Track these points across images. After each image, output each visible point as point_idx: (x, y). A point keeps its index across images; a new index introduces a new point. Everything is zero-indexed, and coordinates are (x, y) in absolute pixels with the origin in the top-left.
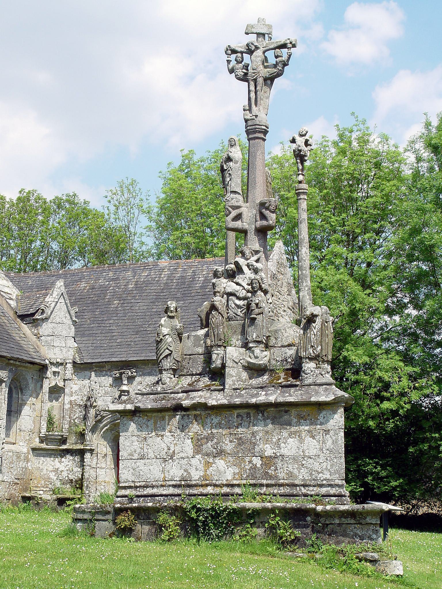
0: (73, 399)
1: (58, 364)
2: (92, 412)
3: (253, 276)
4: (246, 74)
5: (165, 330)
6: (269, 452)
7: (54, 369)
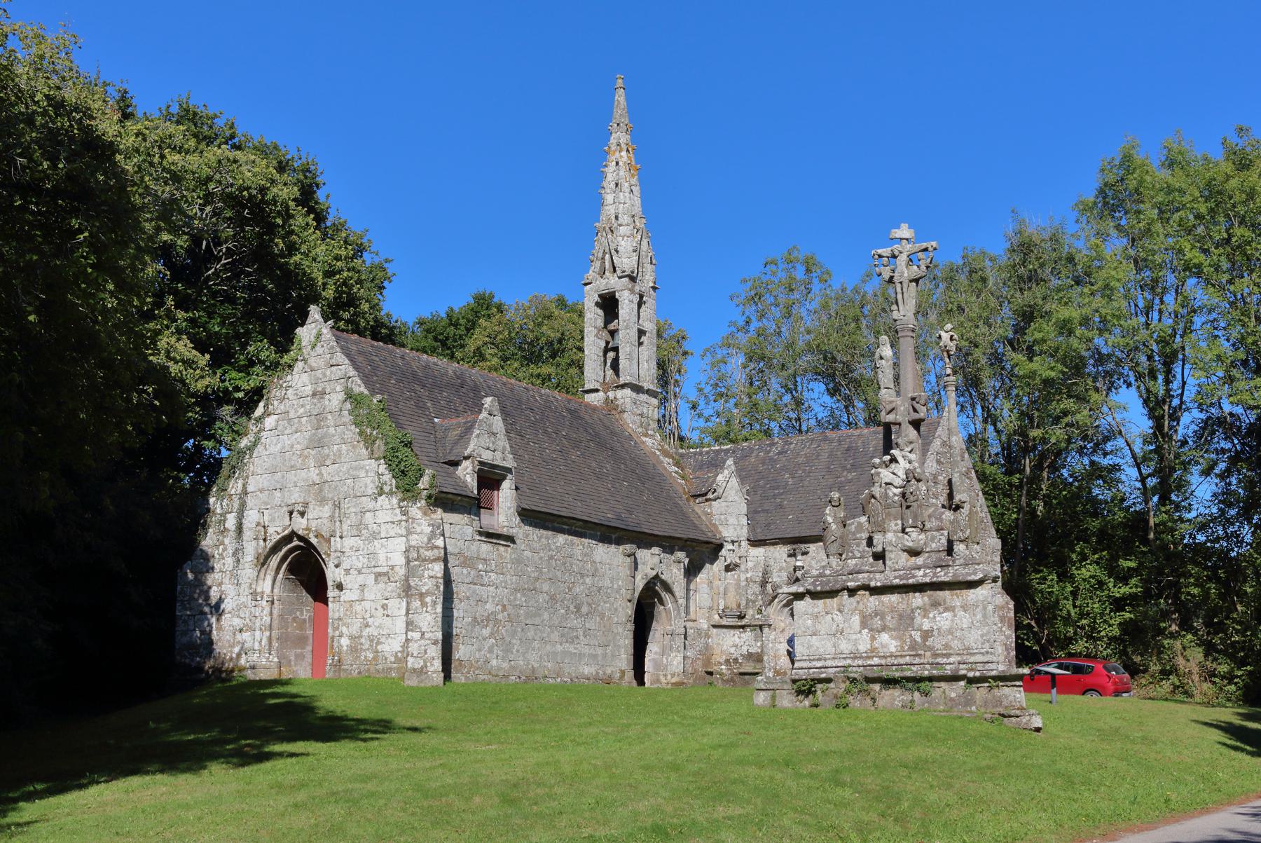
0: (749, 575)
1: (733, 542)
2: (769, 586)
3: (908, 466)
4: (892, 277)
5: (830, 519)
6: (926, 627)
7: (730, 546)
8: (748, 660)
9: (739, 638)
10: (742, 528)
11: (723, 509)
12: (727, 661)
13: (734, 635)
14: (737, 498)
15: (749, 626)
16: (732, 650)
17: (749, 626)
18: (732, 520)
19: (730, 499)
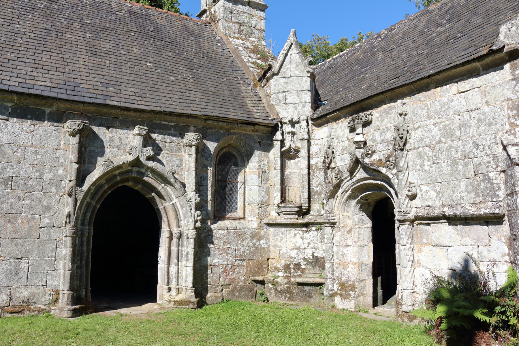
8: (314, 266)
9: (302, 238)
10: (304, 107)
11: (281, 86)
12: (287, 267)
13: (295, 235)
14: (297, 72)
15: (313, 224)
16: (293, 253)
17: (313, 224)
18: (292, 98)
19: (289, 74)
